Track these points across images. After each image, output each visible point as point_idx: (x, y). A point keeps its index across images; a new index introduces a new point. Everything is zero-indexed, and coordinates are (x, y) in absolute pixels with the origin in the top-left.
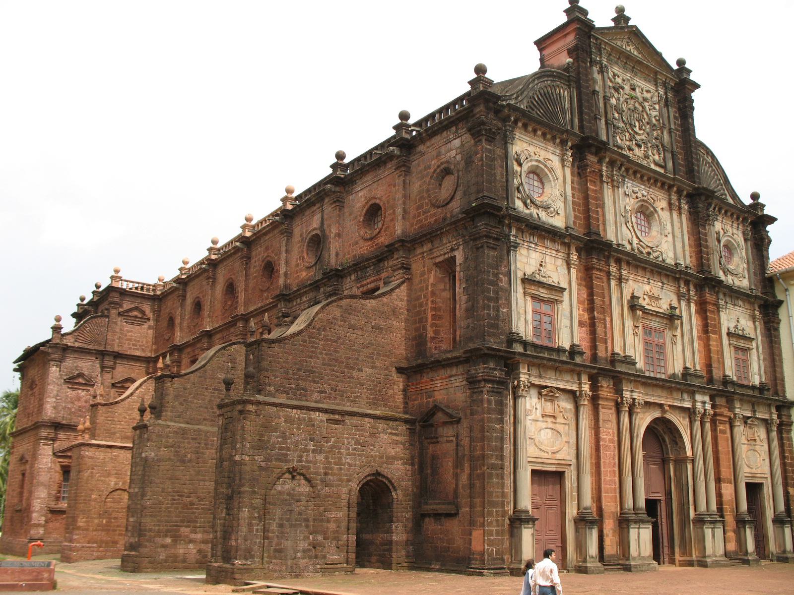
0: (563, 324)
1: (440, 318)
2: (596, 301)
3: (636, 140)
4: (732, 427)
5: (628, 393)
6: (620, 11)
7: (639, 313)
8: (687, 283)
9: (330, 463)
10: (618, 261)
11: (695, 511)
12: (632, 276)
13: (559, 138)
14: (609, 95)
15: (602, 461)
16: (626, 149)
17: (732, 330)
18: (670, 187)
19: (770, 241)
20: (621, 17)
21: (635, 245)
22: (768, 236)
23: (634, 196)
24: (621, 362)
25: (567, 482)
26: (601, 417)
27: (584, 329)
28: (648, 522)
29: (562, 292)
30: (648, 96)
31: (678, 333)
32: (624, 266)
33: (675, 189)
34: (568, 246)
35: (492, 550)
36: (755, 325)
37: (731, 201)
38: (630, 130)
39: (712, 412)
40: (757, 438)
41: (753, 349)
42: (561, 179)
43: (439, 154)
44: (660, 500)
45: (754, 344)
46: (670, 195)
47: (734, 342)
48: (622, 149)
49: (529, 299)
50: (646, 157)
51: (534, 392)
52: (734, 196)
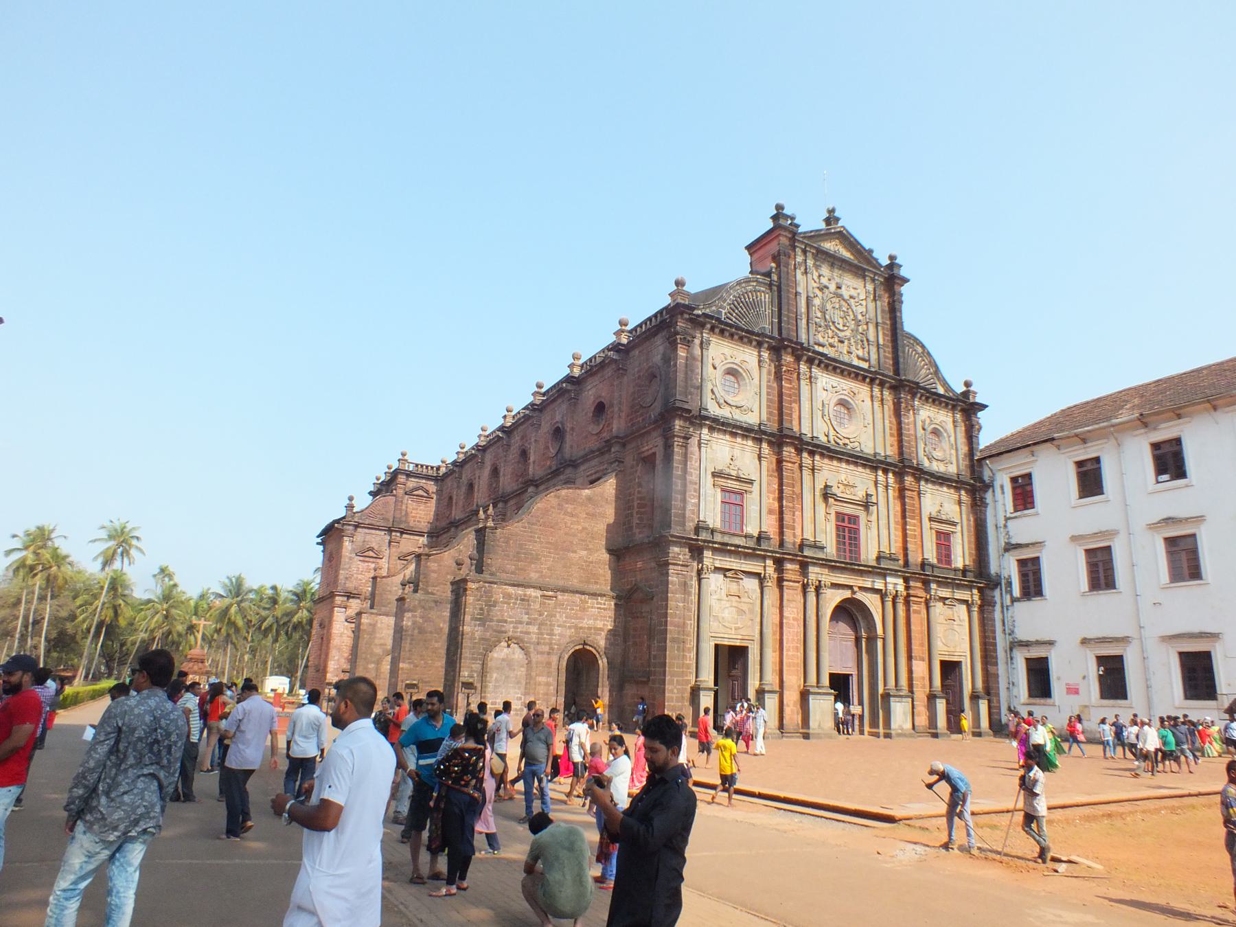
1: (644, 506)
2: (785, 491)
4: (928, 608)
5: (813, 575)
7: (831, 500)
8: (886, 471)
10: (812, 453)
11: (885, 686)
14: (812, 296)
17: (934, 514)
18: (872, 381)
19: (980, 428)
20: (831, 219)
21: (831, 438)
22: (978, 423)
24: (810, 546)
25: (750, 656)
27: (774, 517)
28: (830, 694)
29: (752, 484)
30: (853, 293)
31: (874, 518)
32: (817, 457)
33: (877, 382)
34: (759, 441)
36: (960, 509)
37: (941, 391)
38: (833, 328)
39: (905, 593)
40: (956, 618)
41: (955, 532)
42: (756, 381)
43: (647, 360)
45: (959, 527)
46: (871, 388)
47: (936, 525)
49: (719, 490)
50: (849, 353)
52: (945, 384)
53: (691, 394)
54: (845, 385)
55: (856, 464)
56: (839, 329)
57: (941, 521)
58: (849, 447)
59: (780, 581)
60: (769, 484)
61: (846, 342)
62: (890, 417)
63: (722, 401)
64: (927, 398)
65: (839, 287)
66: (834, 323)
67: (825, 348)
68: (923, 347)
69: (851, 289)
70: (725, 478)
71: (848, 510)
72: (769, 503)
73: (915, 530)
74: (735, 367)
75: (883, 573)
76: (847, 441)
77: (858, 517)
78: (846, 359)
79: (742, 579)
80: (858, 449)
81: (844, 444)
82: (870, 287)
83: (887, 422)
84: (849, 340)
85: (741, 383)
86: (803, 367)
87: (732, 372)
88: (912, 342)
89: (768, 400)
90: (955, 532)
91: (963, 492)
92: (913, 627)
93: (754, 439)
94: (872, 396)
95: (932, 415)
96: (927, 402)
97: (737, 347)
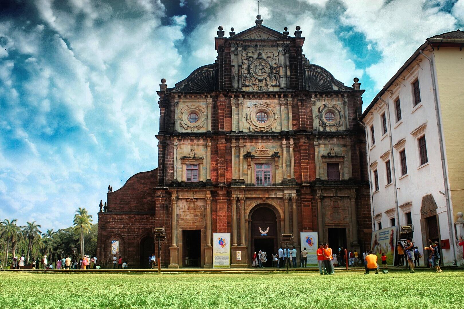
0: (203, 171)
3: (259, 79)
7: (249, 159)
8: (288, 139)
9: (129, 232)
15: (218, 225)
18: (280, 97)
19: (362, 102)
21: (252, 130)
25: (201, 234)
26: (218, 207)
29: (203, 159)
30: (270, 54)
32: (241, 141)
33: (282, 96)
37: (336, 88)
38: (255, 76)
45: (346, 159)
48: (248, 86)
51: (184, 202)
53: (170, 127)
54: (261, 103)
55: (267, 139)
56: (260, 76)
58: (264, 132)
59: (215, 200)
60: (212, 158)
61: (264, 81)
62: (292, 111)
63: (186, 126)
64: (321, 96)
65: (260, 54)
66: (256, 73)
67: (250, 87)
68: (321, 68)
69: (268, 53)
70: (187, 159)
72: (214, 166)
73: (307, 165)
74: (194, 110)
75: (282, 190)
76: (262, 129)
78: (264, 89)
79: (196, 201)
80: (270, 131)
82: (281, 49)
83: (290, 115)
84: (266, 79)
85: (198, 116)
87: (192, 112)
88: (313, 68)
89: (212, 121)
90: (343, 162)
91: (347, 139)
92: (304, 214)
93: (204, 140)
94: (280, 104)
95: (326, 103)
97: (195, 101)
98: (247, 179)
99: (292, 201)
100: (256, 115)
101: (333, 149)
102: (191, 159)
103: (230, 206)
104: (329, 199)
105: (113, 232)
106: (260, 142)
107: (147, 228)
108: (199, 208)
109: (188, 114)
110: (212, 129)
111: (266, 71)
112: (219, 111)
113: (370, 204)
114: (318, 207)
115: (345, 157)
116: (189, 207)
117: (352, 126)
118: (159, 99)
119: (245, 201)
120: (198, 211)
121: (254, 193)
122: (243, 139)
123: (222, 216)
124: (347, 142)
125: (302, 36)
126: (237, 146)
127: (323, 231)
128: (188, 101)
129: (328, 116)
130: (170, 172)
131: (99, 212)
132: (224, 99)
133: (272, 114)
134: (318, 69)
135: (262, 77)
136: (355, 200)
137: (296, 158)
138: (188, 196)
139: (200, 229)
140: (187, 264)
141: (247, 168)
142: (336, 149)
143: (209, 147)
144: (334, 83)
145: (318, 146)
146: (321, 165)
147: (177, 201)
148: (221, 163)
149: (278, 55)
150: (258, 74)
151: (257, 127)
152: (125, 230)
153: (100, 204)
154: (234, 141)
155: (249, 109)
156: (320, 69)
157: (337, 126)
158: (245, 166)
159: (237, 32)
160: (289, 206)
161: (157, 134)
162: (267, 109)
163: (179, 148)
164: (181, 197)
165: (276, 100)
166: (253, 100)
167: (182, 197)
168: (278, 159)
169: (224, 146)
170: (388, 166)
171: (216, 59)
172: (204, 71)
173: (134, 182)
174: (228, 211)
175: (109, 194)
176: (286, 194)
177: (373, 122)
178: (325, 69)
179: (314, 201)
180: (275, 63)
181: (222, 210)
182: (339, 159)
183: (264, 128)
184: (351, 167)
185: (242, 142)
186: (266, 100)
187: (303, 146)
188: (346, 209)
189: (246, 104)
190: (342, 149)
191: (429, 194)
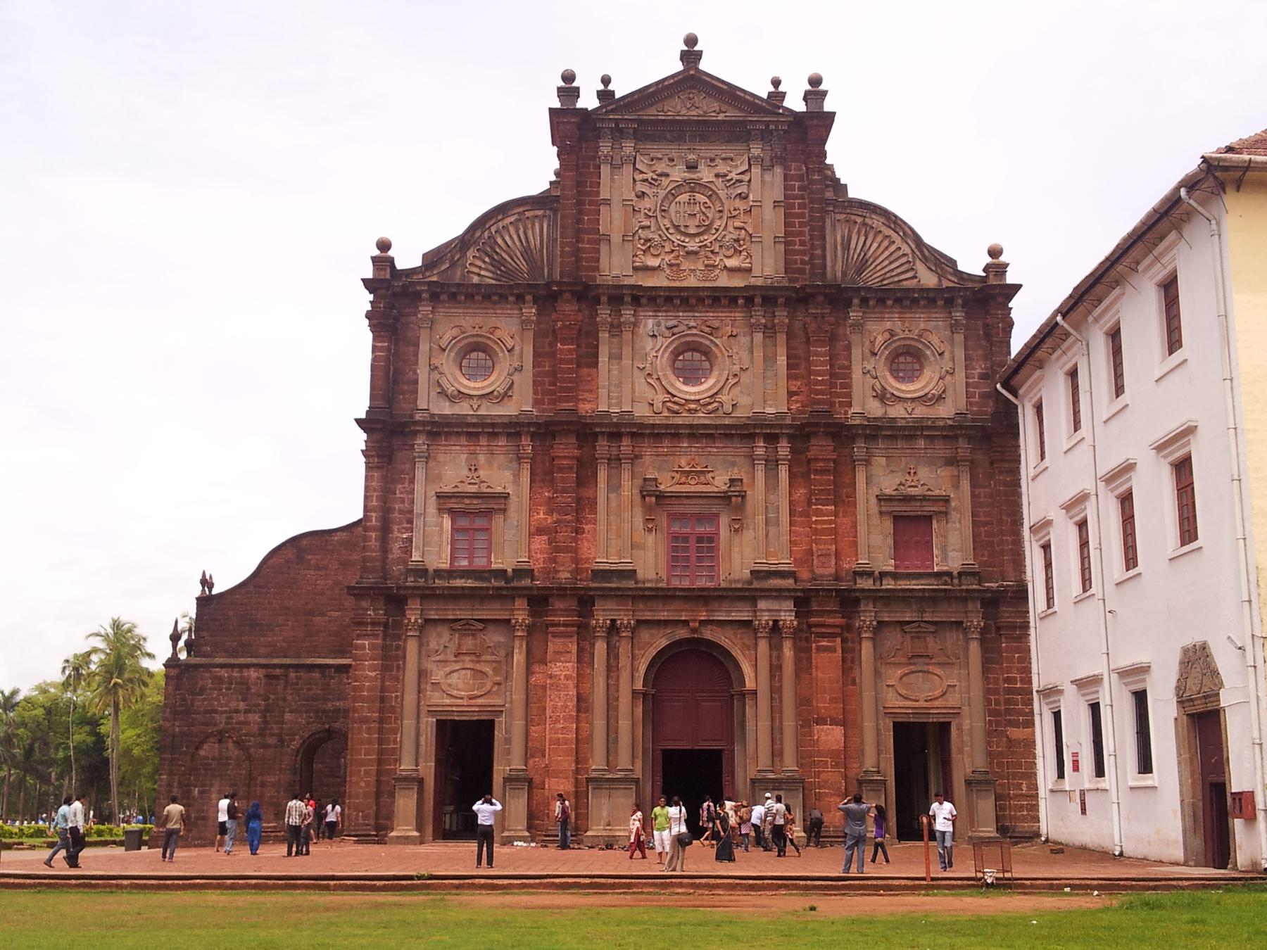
3: (685, 247)
6: (691, 41)
8: (772, 439)
10: (615, 435)
12: (648, 454)
13: (512, 295)
15: (549, 705)
16: (665, 266)
17: (889, 491)
18: (750, 301)
19: (1011, 324)
20: (691, 55)
21: (658, 406)
23: (667, 333)
25: (496, 732)
27: (546, 538)
29: (505, 498)
30: (722, 168)
33: (758, 300)
35: (357, 816)
37: (928, 279)
44: (724, 750)
48: (653, 269)
54: (690, 323)
55: (710, 436)
57: (908, 499)
63: (450, 390)
65: (692, 167)
66: (677, 227)
71: (694, 508)
76: (693, 406)
77: (717, 515)
79: (481, 630)
81: (689, 411)
82: (756, 151)
83: (782, 360)
85: (495, 359)
86: (604, 313)
90: (946, 513)
91: (962, 443)
93: (509, 435)
94: (752, 328)
96: (886, 307)
97: (485, 311)
98: (642, 561)
99: (781, 633)
100: (674, 361)
101: (912, 471)
102: (467, 497)
103: (587, 646)
104: (898, 629)
105: (215, 725)
106: (685, 445)
107: (324, 711)
108: (490, 651)
109: (463, 354)
110: (536, 403)
111: (707, 217)
112: (559, 345)
113: (1029, 646)
114: (863, 652)
115: (952, 496)
116: (460, 646)
117: (977, 399)
118: (371, 302)
119: (634, 630)
120: (486, 661)
121: (664, 605)
122: (632, 437)
123: (562, 677)
124: (959, 450)
125: (828, 106)
126: (613, 457)
127: (878, 730)
128: (461, 311)
129: (902, 367)
130: (399, 535)
131: (169, 660)
132: (573, 308)
133: (723, 354)
134: (873, 216)
135: (697, 240)
136: (981, 634)
137: (796, 497)
138: (458, 613)
139: (491, 718)
140: (447, 827)
141: (642, 527)
142: (924, 474)
143: (525, 458)
144: (925, 260)
145: (868, 462)
146: (875, 520)
147: (422, 628)
148: (563, 512)
149: (749, 170)
150: (682, 229)
151: (676, 399)
152: (255, 718)
153: (171, 631)
154: (605, 443)
155: (649, 344)
156: (880, 215)
157: (930, 400)
158: (639, 521)
159: (621, 89)
160: (771, 649)
161: (363, 416)
162: (707, 343)
163: (430, 461)
164: (433, 615)
165: (737, 314)
166: (666, 311)
167: (437, 617)
168: (740, 499)
169: (572, 458)
170: (1084, 536)
171: (554, 178)
172: (512, 219)
173: (287, 561)
174: (579, 660)
175: (203, 602)
176: (763, 611)
177: (1040, 389)
178: (896, 216)
179: (849, 636)
180: (740, 194)
181: (562, 659)
182: (931, 504)
183: (699, 400)
184: (969, 532)
185: (626, 446)
186: (707, 312)
187: (816, 460)
188: (953, 664)
189: (645, 326)
190: (945, 472)
191: (1198, 638)
